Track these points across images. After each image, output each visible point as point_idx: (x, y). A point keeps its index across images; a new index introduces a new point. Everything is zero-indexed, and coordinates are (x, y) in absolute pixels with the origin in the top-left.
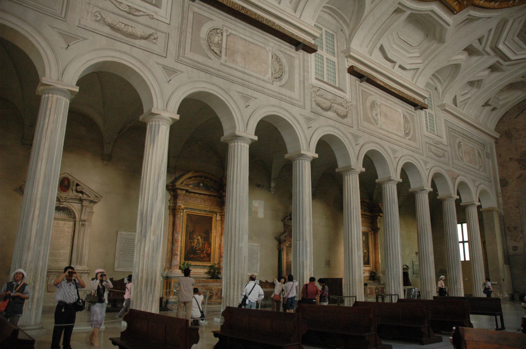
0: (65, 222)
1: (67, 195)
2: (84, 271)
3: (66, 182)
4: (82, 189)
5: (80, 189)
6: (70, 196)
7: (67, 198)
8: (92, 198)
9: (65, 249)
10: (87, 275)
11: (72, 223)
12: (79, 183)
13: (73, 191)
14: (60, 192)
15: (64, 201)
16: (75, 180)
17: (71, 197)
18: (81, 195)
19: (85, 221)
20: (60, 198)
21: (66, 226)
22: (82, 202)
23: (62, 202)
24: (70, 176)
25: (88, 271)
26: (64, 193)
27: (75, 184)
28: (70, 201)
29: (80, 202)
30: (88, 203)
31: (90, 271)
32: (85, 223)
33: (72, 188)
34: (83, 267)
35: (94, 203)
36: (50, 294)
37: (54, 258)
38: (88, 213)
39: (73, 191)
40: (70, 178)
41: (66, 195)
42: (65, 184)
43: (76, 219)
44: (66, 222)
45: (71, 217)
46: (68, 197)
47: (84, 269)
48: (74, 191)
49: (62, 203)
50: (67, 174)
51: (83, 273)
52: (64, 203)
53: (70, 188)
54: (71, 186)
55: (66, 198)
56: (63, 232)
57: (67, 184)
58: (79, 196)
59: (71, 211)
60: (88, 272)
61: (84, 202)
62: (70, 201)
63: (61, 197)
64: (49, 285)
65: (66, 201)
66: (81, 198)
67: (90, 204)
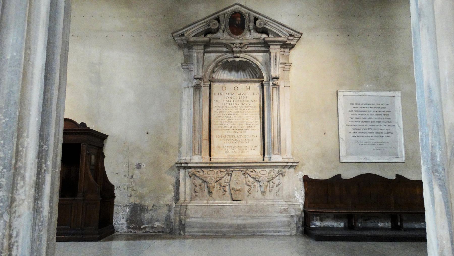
0: (246, 85)
1: (243, 40)
2: (287, 163)
3: (239, 19)
4: (265, 24)
5: (260, 24)
6: (248, 40)
7: (242, 45)
8: (283, 36)
9: (252, 130)
10: (291, 170)
11: (257, 85)
12: (257, 15)
13: (250, 31)
14: (232, 37)
15: (239, 49)
16: (252, 13)
17: (250, 42)
18: (264, 36)
19: (278, 78)
20: (232, 46)
21: (249, 91)
22: (268, 47)
23: (237, 52)
24: (243, 8)
25: (293, 163)
26: (238, 37)
27: (252, 19)
28: (250, 49)
29: (267, 50)
30: (279, 47)
31: (297, 163)
32: (278, 82)
33: (249, 26)
34: (285, 157)
35: (290, 49)
36: (235, 203)
37: (237, 145)
38: (280, 66)
39: (250, 31)
40: (244, 10)
41: (241, 38)
42: (237, 22)
43: (263, 78)
44: (248, 86)
45: (256, 77)
46: (244, 41)
47: (287, 160)
48: (252, 31)
49: (238, 55)
50: (237, 6)
51: (285, 167)
52: (242, 55)
53: (246, 28)
54: (247, 23)
55: (241, 44)
56: (245, 101)
57: (240, 22)
58: (262, 38)
59: (254, 66)
60: (294, 164)
61: (271, 47)
62: (250, 49)
63: (233, 44)
64: (233, 189)
65: (243, 50)
66: (266, 40)
67: (282, 50)
